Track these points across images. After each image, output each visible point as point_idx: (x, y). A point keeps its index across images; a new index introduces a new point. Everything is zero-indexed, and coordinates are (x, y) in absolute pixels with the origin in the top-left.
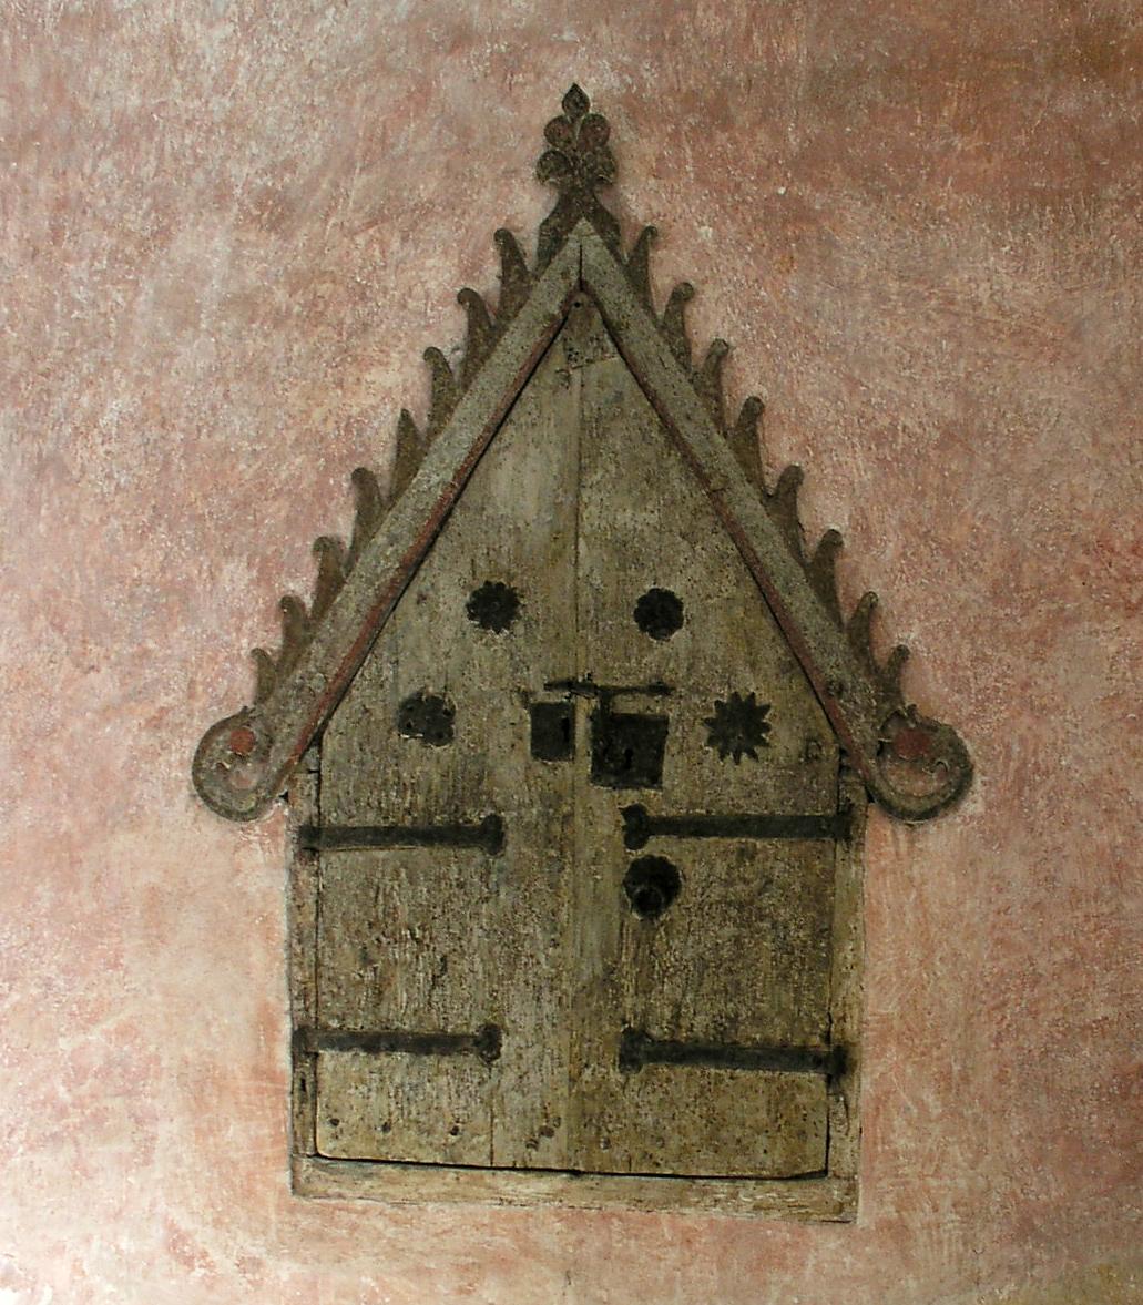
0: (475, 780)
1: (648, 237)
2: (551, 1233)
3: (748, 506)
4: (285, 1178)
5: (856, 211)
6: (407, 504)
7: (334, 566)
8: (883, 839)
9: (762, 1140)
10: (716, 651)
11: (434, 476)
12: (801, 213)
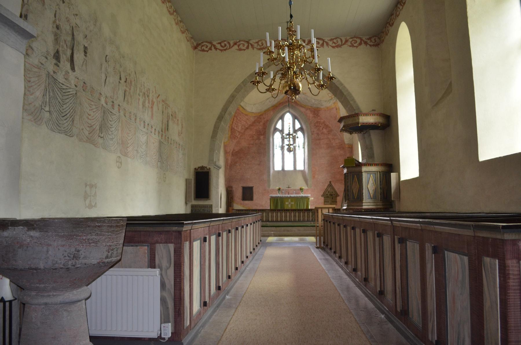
6: (326, 190)
10: (334, 193)
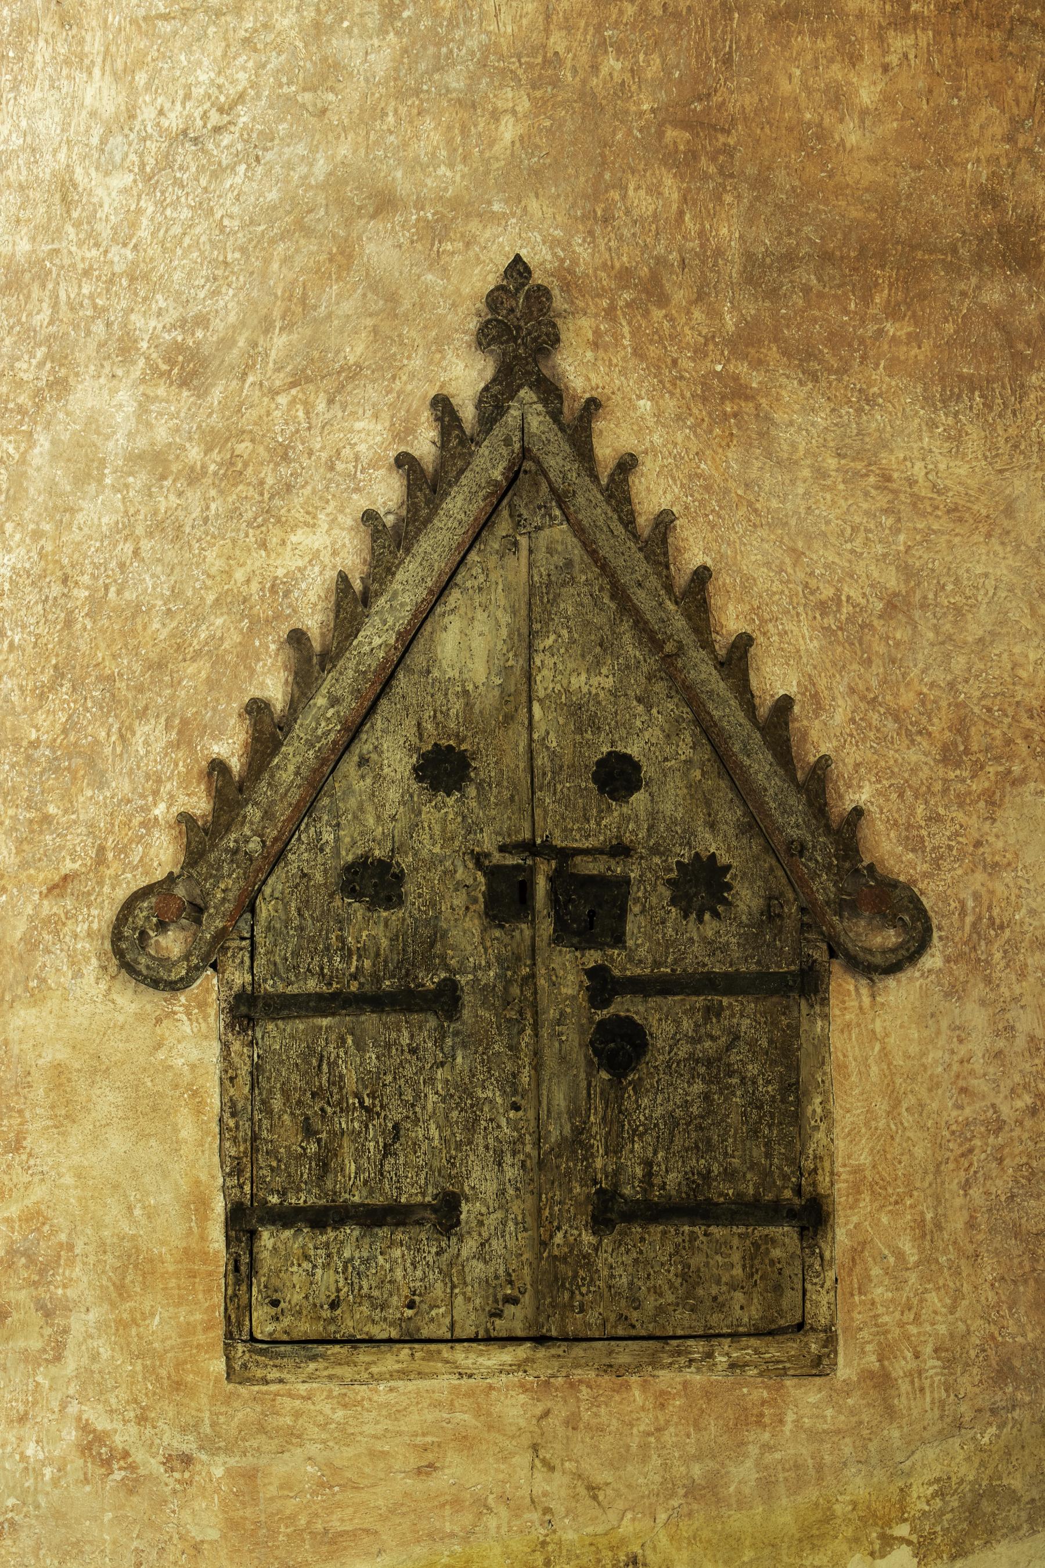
0: (430, 940)
1: (593, 406)
2: (515, 1407)
3: (703, 672)
4: (219, 1365)
5: (791, 390)
6: (349, 662)
7: (267, 731)
8: (847, 992)
9: (739, 1295)
11: (376, 637)
12: (740, 392)
